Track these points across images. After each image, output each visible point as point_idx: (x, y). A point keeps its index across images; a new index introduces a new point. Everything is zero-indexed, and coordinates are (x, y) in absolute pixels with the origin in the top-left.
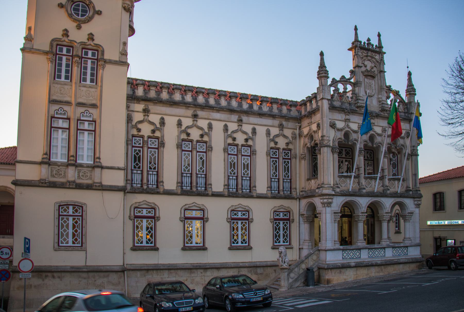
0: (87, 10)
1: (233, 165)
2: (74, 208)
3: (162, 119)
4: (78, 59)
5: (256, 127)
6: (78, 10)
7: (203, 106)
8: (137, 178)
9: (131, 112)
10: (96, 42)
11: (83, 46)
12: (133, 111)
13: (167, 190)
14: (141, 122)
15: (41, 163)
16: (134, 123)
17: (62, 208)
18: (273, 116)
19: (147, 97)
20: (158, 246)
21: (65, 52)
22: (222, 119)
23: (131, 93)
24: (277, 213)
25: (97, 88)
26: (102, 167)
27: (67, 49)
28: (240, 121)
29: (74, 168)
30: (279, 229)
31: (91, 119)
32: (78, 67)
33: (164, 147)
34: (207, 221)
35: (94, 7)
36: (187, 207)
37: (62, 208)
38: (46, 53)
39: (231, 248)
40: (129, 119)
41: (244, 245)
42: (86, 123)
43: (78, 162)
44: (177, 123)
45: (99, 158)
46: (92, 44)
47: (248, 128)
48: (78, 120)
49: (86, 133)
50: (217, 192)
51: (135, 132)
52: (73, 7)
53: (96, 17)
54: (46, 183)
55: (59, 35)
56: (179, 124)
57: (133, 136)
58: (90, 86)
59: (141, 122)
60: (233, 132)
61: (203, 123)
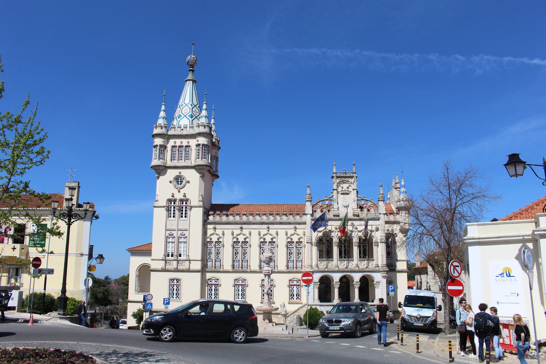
0: (183, 181)
2: (176, 281)
3: (223, 232)
5: (278, 230)
6: (178, 182)
10: (187, 197)
11: (181, 200)
21: (173, 204)
24: (292, 281)
26: (190, 261)
27: (174, 202)
28: (268, 228)
31: (185, 236)
34: (247, 286)
36: (236, 278)
45: (189, 256)
46: (185, 198)
48: (179, 237)
49: (183, 243)
50: (253, 270)
54: (163, 269)
56: (233, 234)
58: (185, 220)
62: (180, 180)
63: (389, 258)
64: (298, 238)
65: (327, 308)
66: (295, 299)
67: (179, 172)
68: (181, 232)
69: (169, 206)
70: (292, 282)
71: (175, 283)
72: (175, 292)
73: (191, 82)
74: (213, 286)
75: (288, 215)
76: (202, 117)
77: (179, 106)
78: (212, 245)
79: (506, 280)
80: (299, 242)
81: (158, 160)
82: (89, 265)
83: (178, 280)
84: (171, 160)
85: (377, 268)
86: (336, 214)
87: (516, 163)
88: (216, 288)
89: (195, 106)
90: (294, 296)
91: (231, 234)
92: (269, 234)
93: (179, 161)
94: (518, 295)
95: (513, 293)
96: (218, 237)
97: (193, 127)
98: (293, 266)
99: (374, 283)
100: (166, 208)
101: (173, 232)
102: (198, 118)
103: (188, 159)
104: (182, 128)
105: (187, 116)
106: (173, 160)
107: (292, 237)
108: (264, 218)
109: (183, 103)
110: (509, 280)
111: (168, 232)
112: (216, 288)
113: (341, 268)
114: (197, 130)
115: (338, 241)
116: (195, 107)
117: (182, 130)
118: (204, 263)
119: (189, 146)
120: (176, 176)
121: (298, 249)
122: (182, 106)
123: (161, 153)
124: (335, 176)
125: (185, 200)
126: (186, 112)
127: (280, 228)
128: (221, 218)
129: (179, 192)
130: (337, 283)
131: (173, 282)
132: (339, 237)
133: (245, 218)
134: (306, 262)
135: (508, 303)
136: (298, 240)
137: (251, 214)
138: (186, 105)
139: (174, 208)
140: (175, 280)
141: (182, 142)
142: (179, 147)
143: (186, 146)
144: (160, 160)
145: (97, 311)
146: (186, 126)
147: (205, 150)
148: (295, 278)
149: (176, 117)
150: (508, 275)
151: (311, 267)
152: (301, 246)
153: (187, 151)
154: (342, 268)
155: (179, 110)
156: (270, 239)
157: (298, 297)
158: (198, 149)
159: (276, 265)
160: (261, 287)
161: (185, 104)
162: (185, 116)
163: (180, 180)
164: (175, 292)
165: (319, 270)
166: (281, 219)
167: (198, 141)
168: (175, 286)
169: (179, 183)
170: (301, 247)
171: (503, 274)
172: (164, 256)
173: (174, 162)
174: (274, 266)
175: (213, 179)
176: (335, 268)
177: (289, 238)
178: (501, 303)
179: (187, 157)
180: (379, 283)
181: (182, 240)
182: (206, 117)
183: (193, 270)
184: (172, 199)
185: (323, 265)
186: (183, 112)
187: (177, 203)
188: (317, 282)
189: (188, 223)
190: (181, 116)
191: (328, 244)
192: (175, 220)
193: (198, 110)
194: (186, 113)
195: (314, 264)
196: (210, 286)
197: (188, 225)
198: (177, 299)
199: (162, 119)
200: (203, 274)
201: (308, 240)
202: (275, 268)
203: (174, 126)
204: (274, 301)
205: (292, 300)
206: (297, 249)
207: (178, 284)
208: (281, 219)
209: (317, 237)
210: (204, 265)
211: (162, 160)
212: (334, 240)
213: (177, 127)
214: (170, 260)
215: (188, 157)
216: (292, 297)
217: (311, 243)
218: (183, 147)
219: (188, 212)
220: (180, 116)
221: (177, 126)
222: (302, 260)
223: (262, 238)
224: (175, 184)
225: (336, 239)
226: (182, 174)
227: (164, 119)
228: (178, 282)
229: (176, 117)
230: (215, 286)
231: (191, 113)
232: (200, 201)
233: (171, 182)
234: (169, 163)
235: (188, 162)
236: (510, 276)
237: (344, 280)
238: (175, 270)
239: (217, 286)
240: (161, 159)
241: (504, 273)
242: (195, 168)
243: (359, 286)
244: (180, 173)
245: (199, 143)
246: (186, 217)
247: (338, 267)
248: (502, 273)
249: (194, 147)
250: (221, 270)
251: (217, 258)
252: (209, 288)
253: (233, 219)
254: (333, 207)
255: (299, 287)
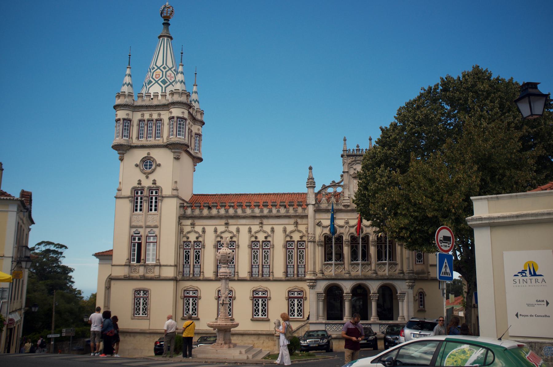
1: (266, 257)
2: (143, 292)
3: (204, 229)
4: (146, 198)
6: (147, 165)
7: (232, 216)
8: (187, 270)
9: (183, 226)
12: (184, 225)
13: (206, 278)
14: (189, 232)
15: (125, 265)
16: (184, 233)
17: (137, 292)
18: (289, 217)
19: (193, 214)
20: (199, 317)
22: (247, 224)
23: (183, 213)
25: (158, 215)
26: (160, 266)
28: (261, 223)
29: (143, 267)
30: (258, 305)
31: (154, 235)
32: (147, 203)
33: (204, 248)
34: (234, 299)
35: (156, 162)
37: (137, 292)
38: (128, 197)
39: (253, 320)
40: (181, 231)
41: (264, 317)
42: (152, 238)
43: (147, 263)
44: (214, 230)
45: (159, 260)
47: (267, 228)
48: (147, 236)
49: (152, 244)
50: (242, 278)
51: (185, 239)
52: (144, 164)
53: (158, 168)
55: (136, 185)
56: (216, 231)
57: (184, 242)
59: (189, 232)
60: (256, 233)
61: (233, 229)
62: (148, 164)
63: (420, 262)
64: (300, 237)
65: (335, 328)
66: (296, 317)
67: (147, 153)
68: (149, 229)
69: (135, 196)
70: (292, 294)
71: (142, 295)
72: (141, 307)
73: (166, 38)
74: (191, 299)
75: (287, 206)
76: (176, 82)
77: (150, 69)
78: (190, 245)
79: (529, 281)
80: (301, 242)
81: (121, 137)
82: (13, 271)
83: (146, 292)
84: (138, 138)
85: (402, 275)
86: (346, 204)
87: (532, 98)
88: (194, 301)
89: (170, 69)
90: (294, 312)
91: (214, 232)
92: (263, 232)
93: (148, 139)
94: (547, 303)
95: (540, 301)
96: (197, 235)
97: (166, 95)
98: (294, 272)
99: (397, 295)
100: (130, 199)
101: (140, 230)
102: (173, 84)
103: (159, 136)
104: (152, 97)
105: (159, 82)
106: (140, 138)
107: (292, 235)
108: (257, 211)
109: (154, 66)
110: (533, 281)
111: (134, 230)
112: (194, 301)
113: (354, 274)
114: (170, 99)
115: (349, 240)
116: (170, 71)
117: (152, 99)
118: (179, 270)
119: (161, 120)
120: (143, 158)
121: (300, 251)
122: (153, 69)
123: (125, 129)
124: (345, 154)
125: (155, 189)
126: (157, 76)
127: (277, 223)
128: (201, 212)
129: (147, 177)
130: (348, 295)
131: (138, 294)
132: (350, 234)
133: (231, 211)
134: (310, 267)
135: (533, 316)
136: (300, 238)
137: (241, 206)
138: (159, 68)
139: (141, 199)
140: (142, 292)
141: (151, 115)
142: (148, 120)
143: (157, 120)
144: (124, 138)
145: (64, 335)
146: (157, 94)
147: (180, 124)
148: (295, 288)
149: (145, 83)
150: (533, 274)
151: (314, 273)
152: (303, 246)
153: (158, 126)
154: (356, 274)
155: (149, 75)
156: (264, 238)
157: (300, 314)
158: (172, 123)
159: (271, 271)
160: (251, 299)
161: (157, 66)
162: (157, 82)
163: (148, 164)
164: (141, 307)
165: (324, 277)
166: (278, 211)
167: (171, 112)
168: (142, 299)
169: (148, 167)
170: (304, 247)
171: (525, 272)
172: (127, 261)
173: (141, 140)
174: (269, 272)
175: (194, 163)
176: (345, 275)
177: (288, 236)
178: (523, 316)
179: (159, 134)
180: (404, 295)
181: (152, 240)
182: (182, 83)
183: (164, 278)
184: (139, 187)
185: (329, 271)
186: (154, 77)
187: (146, 193)
188: (322, 294)
189: (158, 218)
190: (152, 82)
191: (338, 244)
192: (143, 215)
193: (174, 75)
194: (157, 78)
195: (318, 270)
196: (186, 299)
197: (158, 220)
198: (144, 316)
199: (126, 86)
200: (178, 284)
201: (310, 238)
202: (270, 275)
203: (142, 95)
204: (270, 317)
205: (292, 317)
206: (299, 250)
207: (145, 296)
208: (278, 211)
209: (322, 234)
210: (179, 272)
211: (126, 138)
212: (344, 239)
213: (146, 96)
214: (135, 266)
215: (159, 134)
216: (292, 314)
217: (314, 242)
218: (153, 120)
219: (159, 204)
220: (150, 82)
221: (146, 95)
222: (305, 265)
223: (253, 236)
224: (142, 168)
225: (347, 236)
226: (151, 155)
227: (129, 85)
228: (145, 294)
229: (146, 84)
230: (193, 299)
231: (164, 78)
232: (174, 190)
233: (137, 166)
234: (135, 142)
235: (159, 140)
236: (535, 275)
237: (359, 291)
238: (142, 278)
239: (196, 299)
240: (125, 136)
241: (526, 270)
242: (167, 147)
243: (377, 298)
244: (149, 154)
245: (173, 115)
246: (156, 210)
247: (349, 273)
248: (523, 271)
249: (166, 121)
250: (201, 278)
251: (196, 263)
252: (185, 301)
253: (217, 213)
254: (343, 195)
255: (301, 300)
